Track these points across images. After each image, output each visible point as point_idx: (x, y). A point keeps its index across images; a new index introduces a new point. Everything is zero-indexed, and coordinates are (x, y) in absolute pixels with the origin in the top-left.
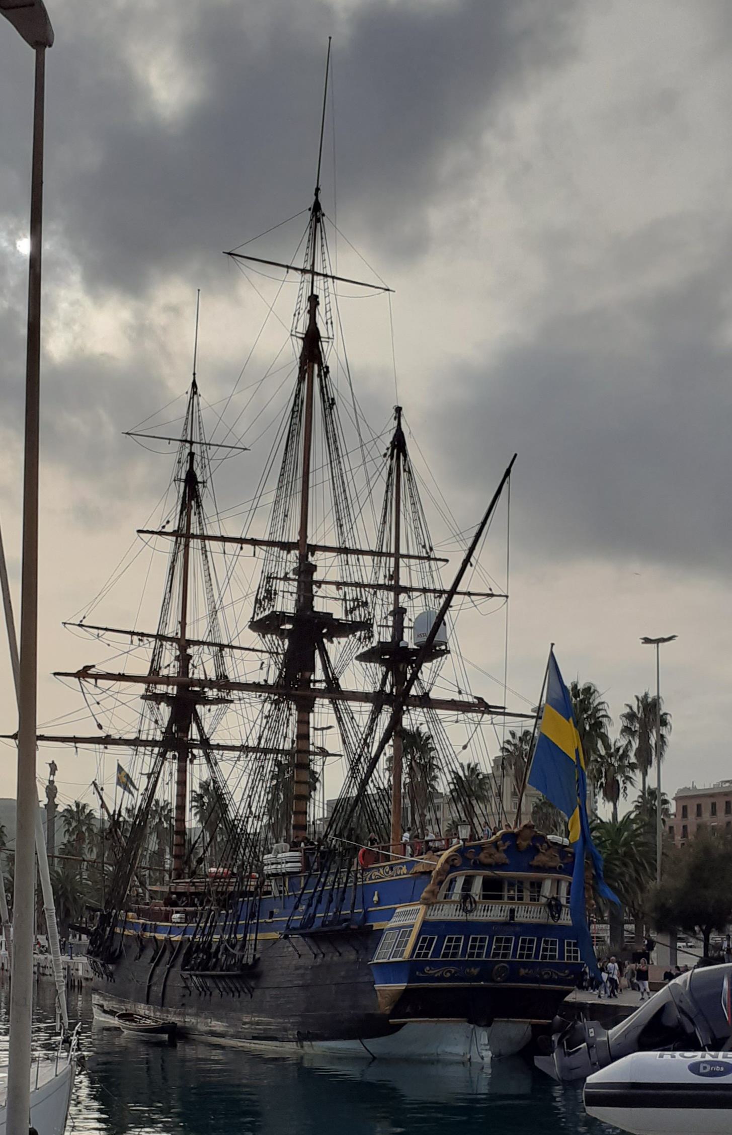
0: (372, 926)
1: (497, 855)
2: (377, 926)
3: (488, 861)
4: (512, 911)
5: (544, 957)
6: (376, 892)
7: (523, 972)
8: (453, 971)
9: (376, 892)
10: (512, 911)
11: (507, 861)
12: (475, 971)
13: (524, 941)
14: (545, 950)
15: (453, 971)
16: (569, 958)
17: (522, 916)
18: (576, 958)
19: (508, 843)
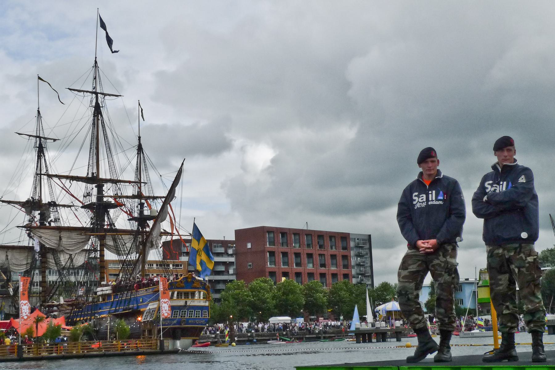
0: (140, 310)
1: (181, 284)
2: (142, 310)
3: (178, 286)
4: (186, 302)
5: (196, 316)
6: (141, 299)
7: (190, 321)
8: (168, 322)
9: (141, 299)
10: (186, 302)
11: (185, 286)
12: (175, 322)
13: (190, 312)
14: (197, 314)
15: (168, 322)
16: (204, 316)
17: (190, 303)
18: (206, 316)
19: (185, 280)
